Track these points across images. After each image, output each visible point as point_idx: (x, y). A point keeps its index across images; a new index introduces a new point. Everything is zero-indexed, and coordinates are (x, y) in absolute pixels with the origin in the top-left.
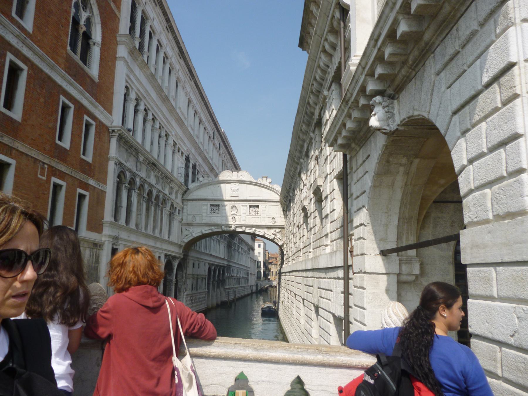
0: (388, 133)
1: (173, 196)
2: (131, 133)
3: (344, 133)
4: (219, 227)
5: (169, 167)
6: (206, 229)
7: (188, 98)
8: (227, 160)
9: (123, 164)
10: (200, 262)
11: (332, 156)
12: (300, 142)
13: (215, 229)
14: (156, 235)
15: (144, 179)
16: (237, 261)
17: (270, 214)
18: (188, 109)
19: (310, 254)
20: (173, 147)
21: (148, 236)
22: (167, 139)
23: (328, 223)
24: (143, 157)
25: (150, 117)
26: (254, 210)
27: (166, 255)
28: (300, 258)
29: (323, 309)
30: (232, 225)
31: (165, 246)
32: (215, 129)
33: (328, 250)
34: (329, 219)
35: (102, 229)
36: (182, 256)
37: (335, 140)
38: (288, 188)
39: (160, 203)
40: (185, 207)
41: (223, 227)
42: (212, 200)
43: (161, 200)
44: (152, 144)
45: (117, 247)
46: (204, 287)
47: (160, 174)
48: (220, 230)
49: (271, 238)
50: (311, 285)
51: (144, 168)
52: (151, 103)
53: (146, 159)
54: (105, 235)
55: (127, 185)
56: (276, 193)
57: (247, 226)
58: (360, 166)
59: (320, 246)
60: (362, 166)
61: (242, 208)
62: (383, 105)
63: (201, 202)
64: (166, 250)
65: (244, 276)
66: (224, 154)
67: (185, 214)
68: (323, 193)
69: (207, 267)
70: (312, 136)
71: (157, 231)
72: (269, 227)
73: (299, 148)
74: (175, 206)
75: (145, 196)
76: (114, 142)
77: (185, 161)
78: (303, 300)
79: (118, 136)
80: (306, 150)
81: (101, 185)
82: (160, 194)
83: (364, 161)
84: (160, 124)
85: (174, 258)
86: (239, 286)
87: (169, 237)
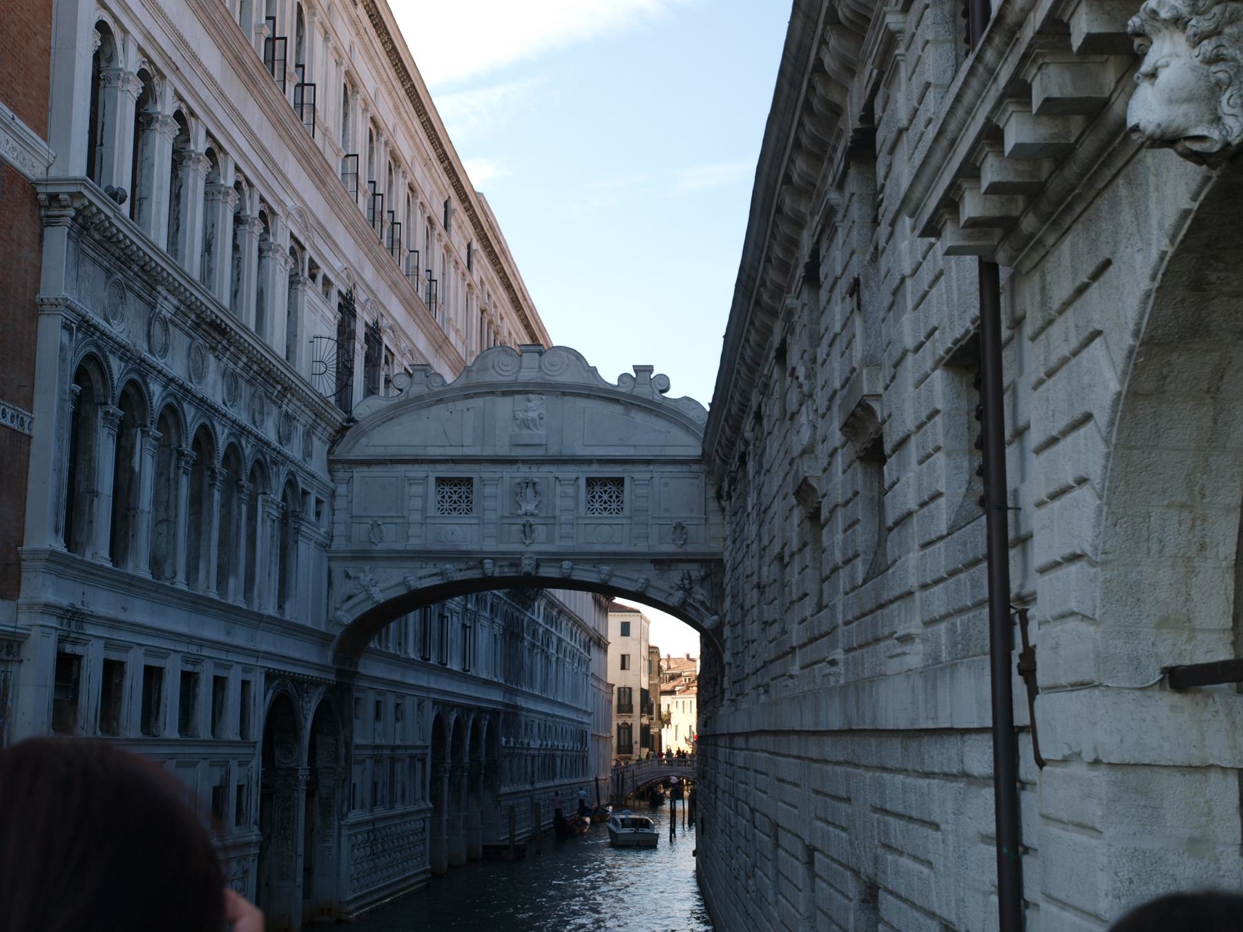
0: (1211, 155)
1: (294, 450)
2: (125, 208)
3: (991, 172)
4: (471, 564)
5: (277, 339)
6: (423, 572)
7: (343, 69)
8: (500, 309)
9: (96, 328)
10: (403, 696)
11: (926, 275)
12: (784, 228)
13: (456, 573)
14: (230, 601)
15: (181, 386)
16: (544, 688)
17: (666, 510)
18: (346, 115)
20: (291, 260)
21: (199, 605)
22: (267, 230)
24: (175, 302)
25: (200, 145)
26: (605, 497)
27: (270, 676)
28: (790, 683)
29: (898, 897)
30: (522, 553)
31: (266, 642)
32: (452, 192)
33: (915, 656)
34: (916, 531)
35: (19, 583)
36: (332, 677)
37: (951, 203)
38: (734, 409)
39: (244, 479)
40: (342, 489)
41: (488, 564)
43: (249, 464)
44: (208, 247)
45: (79, 650)
46: (419, 795)
47: (241, 364)
48: (475, 574)
50: (842, 793)
51: (180, 341)
52: (204, 93)
53: (187, 306)
54: (30, 606)
55: (113, 409)
57: (579, 558)
58: (1061, 312)
59: (877, 640)
60: (1070, 312)
62: (1190, 31)
63: (401, 469)
64: (268, 655)
65: (568, 745)
66: (487, 286)
67: (340, 516)
68: (886, 427)
69: (430, 715)
70: (833, 202)
71: (235, 584)
72: (662, 562)
73: (778, 251)
74: (301, 485)
75: (187, 448)
76: (58, 241)
77: (339, 316)
78: (811, 851)
79: (74, 219)
80: (807, 260)
81: (9, 412)
82: (244, 442)
83: (1081, 290)
84: (238, 169)
85: (301, 683)
86: (552, 784)
87: (281, 607)
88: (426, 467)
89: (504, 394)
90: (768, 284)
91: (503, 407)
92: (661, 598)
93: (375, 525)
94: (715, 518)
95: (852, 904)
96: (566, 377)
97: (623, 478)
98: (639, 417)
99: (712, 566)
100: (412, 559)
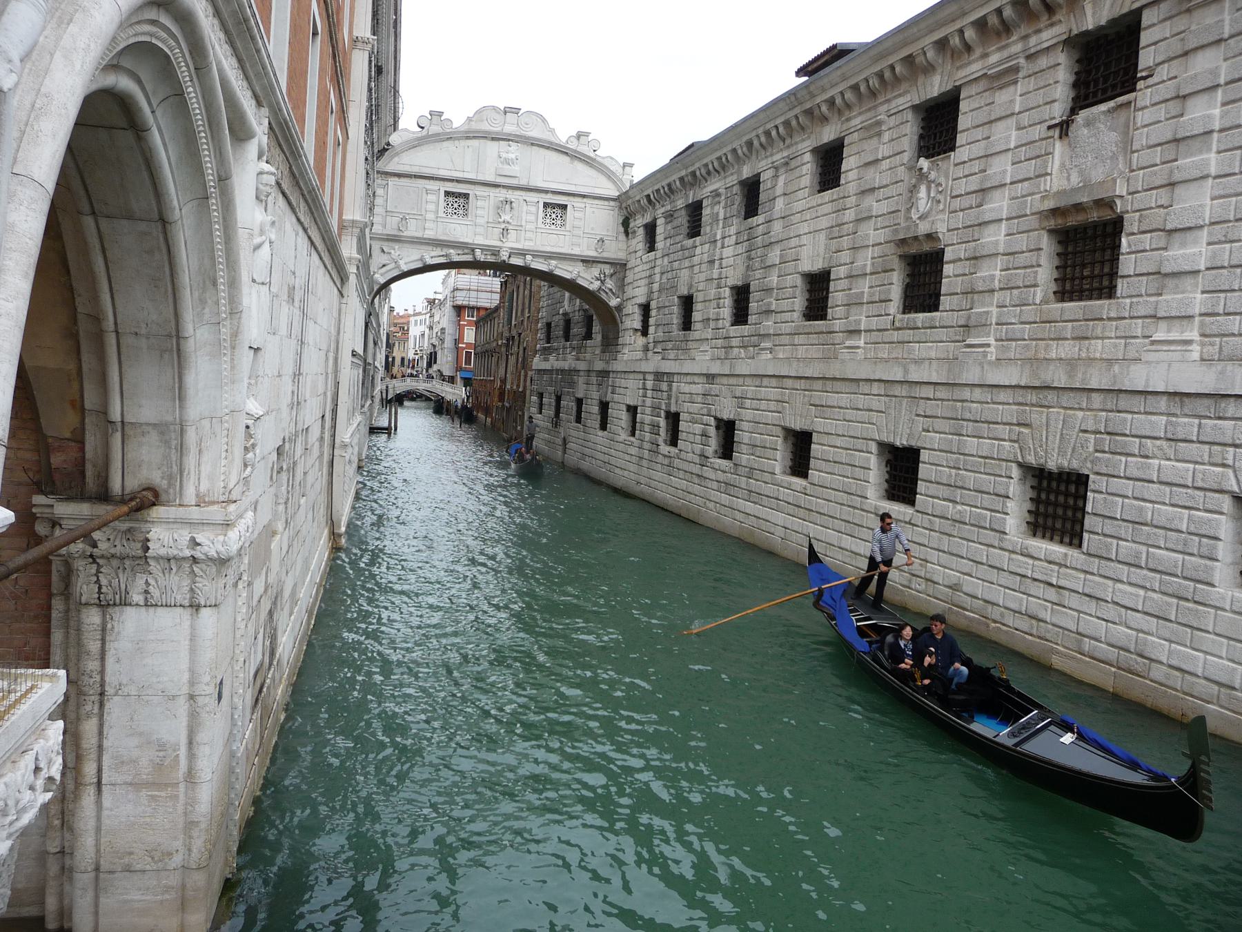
4: (466, 251)
6: (433, 254)
17: (592, 229)
19: (987, 350)
23: (1195, 292)
26: (554, 216)
30: (501, 248)
40: (380, 192)
41: (478, 252)
42: (452, 181)
48: (469, 258)
49: (591, 287)
56: (609, 178)
57: (537, 254)
59: (1087, 338)
61: (525, 208)
72: (587, 262)
88: (438, 183)
89: (493, 139)
90: (838, 101)
91: (492, 148)
92: (585, 284)
93: (404, 219)
94: (622, 237)
95: (1012, 481)
96: (535, 133)
97: (566, 206)
98: (580, 166)
99: (620, 268)
100: (428, 244)
